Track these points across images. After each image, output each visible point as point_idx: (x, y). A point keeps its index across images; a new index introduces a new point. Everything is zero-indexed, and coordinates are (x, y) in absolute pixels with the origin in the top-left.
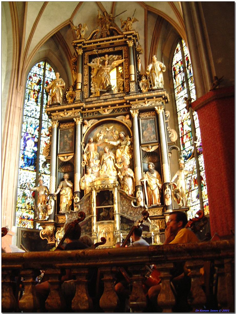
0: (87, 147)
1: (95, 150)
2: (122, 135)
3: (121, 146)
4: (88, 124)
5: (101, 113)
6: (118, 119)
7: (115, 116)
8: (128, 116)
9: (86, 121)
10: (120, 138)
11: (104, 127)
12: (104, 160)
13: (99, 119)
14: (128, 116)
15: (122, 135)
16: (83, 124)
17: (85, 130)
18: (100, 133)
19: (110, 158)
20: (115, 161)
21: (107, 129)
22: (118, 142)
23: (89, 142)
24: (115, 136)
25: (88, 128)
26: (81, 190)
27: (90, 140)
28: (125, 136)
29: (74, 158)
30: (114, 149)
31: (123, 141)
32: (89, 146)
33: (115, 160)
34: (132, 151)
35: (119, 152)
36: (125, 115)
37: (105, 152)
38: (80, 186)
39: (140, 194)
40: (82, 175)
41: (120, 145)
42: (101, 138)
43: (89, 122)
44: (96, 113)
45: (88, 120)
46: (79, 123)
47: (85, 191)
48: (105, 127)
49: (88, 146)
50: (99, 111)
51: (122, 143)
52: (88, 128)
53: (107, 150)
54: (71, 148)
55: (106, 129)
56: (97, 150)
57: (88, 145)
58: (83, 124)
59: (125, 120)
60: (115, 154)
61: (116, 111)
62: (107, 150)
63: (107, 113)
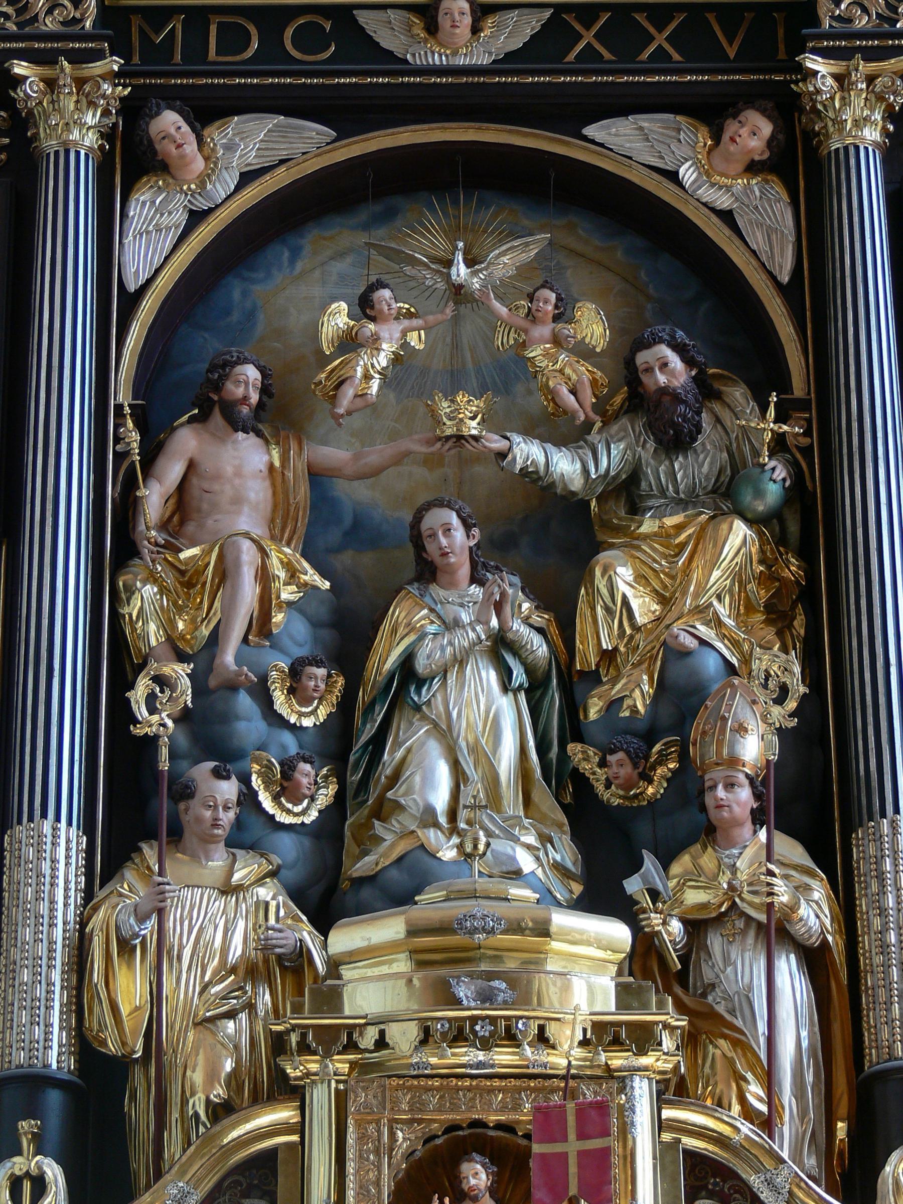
0: (172, 471)
1: (280, 521)
2: (668, 368)
3: (635, 509)
4: (199, 164)
5: (388, 40)
6: (627, 143)
7: (574, 112)
8: (754, 132)
9: (170, 122)
10: (631, 397)
11: (424, 235)
12: (421, 665)
13: (343, 113)
14: (754, 132)
15: (669, 368)
16: (131, 159)
17: (153, 242)
18: (365, 307)
19: (500, 647)
21: (461, 271)
22: (611, 457)
23: (210, 404)
25: (196, 217)
26: (84, 1046)
27: (218, 387)
28: (706, 389)
31: (676, 441)
32: (206, 465)
33: (555, 697)
35: (623, 581)
36: (712, 112)
37: (428, 571)
38: (77, 1007)
40: (108, 860)
41: (627, 491)
43: (218, 135)
44: (309, 39)
45: (204, 112)
46: (80, 130)
47: (140, 1080)
48: (441, 243)
49: (191, 466)
50: (364, 18)
51: (656, 472)
52: (196, 217)
53: (455, 538)
55: (449, 263)
56: (319, 518)
57: (186, 442)
58: (131, 159)
59: (707, 174)
60: (560, 609)
61: (588, 37)
62: (455, 538)
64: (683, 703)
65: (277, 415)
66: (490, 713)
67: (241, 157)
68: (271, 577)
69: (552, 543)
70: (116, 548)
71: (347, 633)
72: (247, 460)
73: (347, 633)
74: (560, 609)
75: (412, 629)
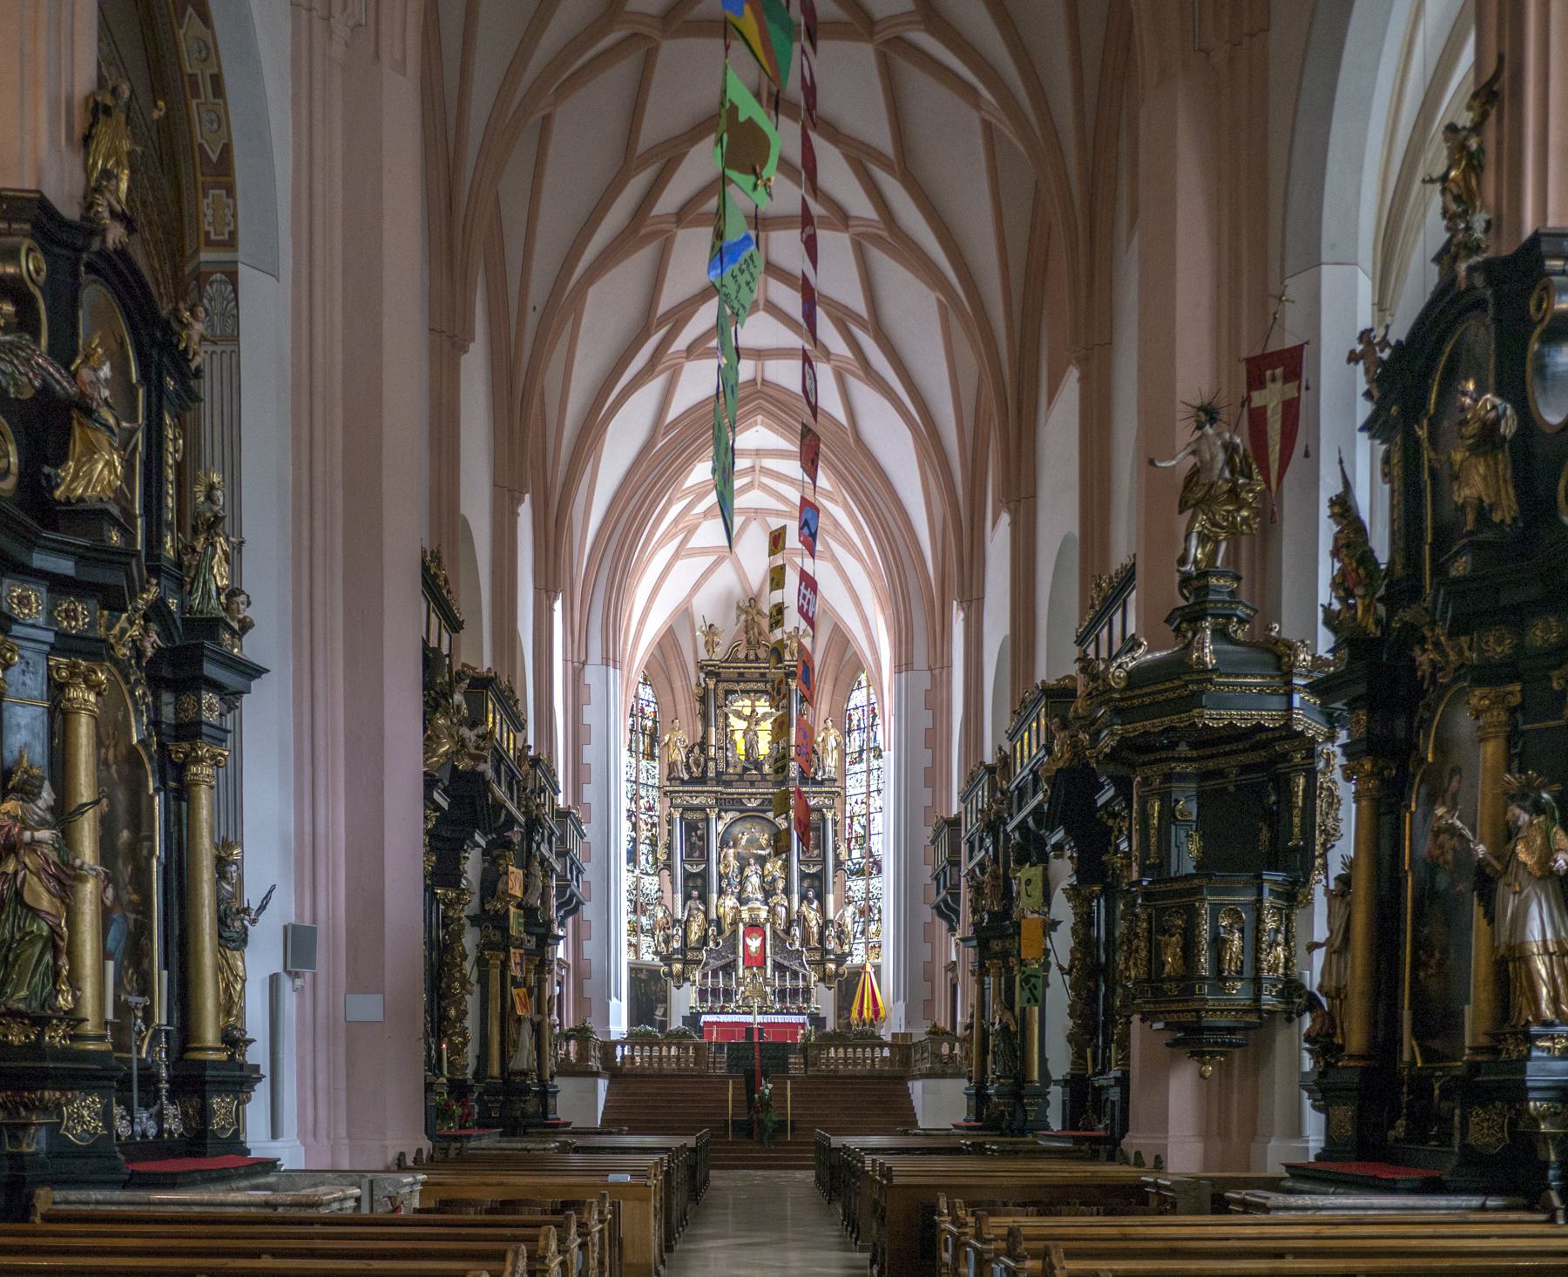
6: (770, 815)
7: (764, 811)
13: (741, 811)
17: (721, 828)
20: (762, 877)
24: (764, 842)
29: (707, 871)
30: (762, 861)
34: (787, 866)
35: (768, 866)
39: (796, 931)
42: (743, 842)
54: (702, 855)
56: (738, 857)
60: (763, 868)
63: (753, 804)
64: (774, 880)
65: (735, 846)
66: (755, 880)
67: (728, 817)
68: (734, 863)
69: (762, 861)
70: (719, 863)
71: (742, 870)
72: (731, 851)
73: (742, 870)
74: (763, 868)
75: (747, 871)
